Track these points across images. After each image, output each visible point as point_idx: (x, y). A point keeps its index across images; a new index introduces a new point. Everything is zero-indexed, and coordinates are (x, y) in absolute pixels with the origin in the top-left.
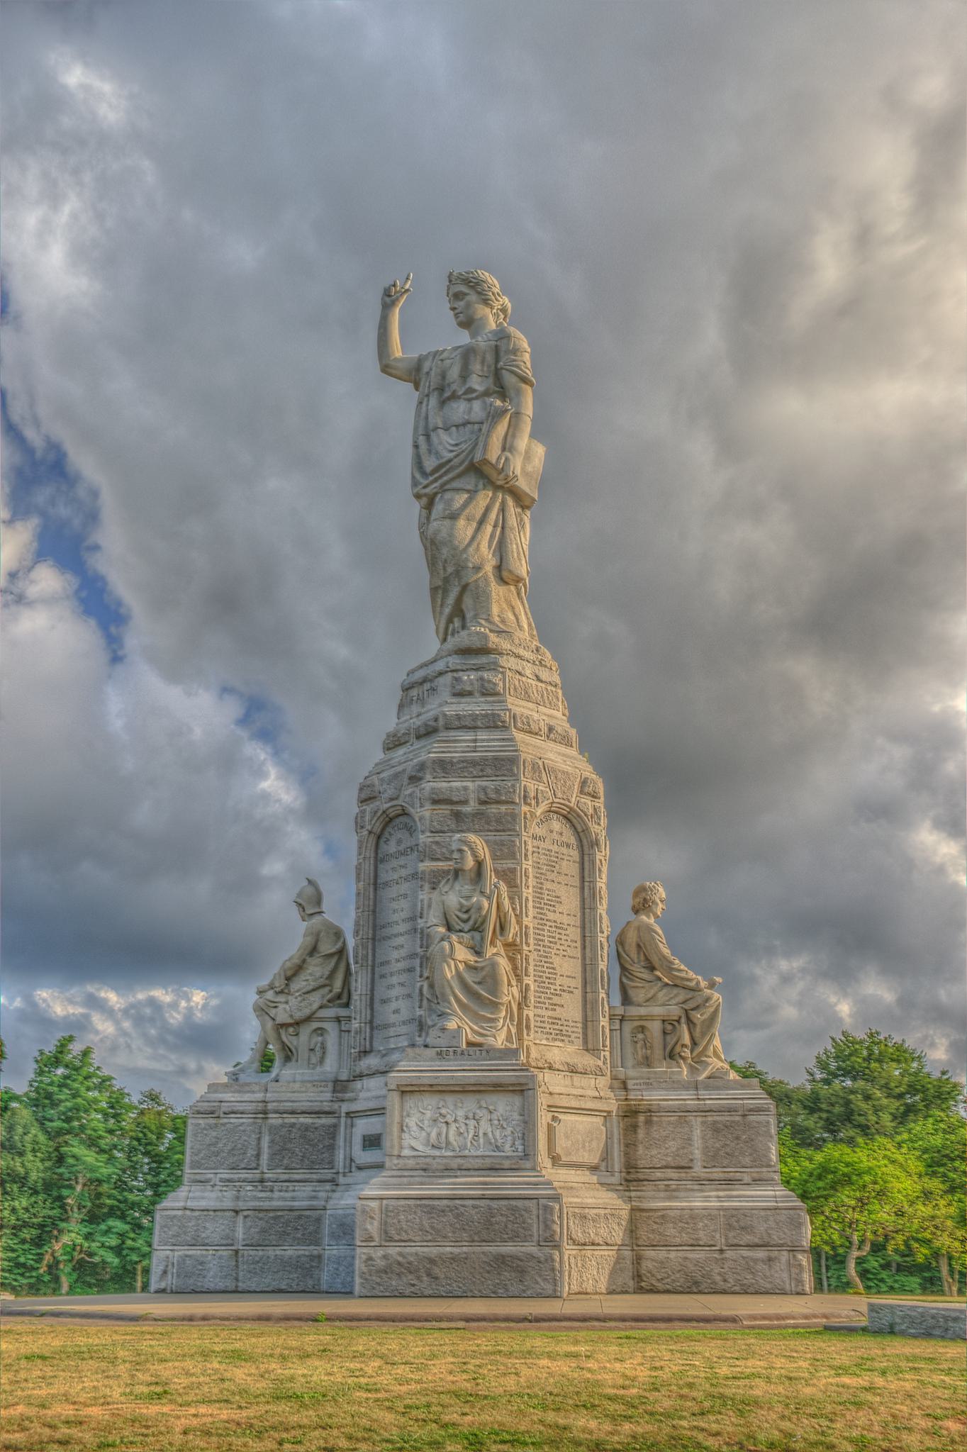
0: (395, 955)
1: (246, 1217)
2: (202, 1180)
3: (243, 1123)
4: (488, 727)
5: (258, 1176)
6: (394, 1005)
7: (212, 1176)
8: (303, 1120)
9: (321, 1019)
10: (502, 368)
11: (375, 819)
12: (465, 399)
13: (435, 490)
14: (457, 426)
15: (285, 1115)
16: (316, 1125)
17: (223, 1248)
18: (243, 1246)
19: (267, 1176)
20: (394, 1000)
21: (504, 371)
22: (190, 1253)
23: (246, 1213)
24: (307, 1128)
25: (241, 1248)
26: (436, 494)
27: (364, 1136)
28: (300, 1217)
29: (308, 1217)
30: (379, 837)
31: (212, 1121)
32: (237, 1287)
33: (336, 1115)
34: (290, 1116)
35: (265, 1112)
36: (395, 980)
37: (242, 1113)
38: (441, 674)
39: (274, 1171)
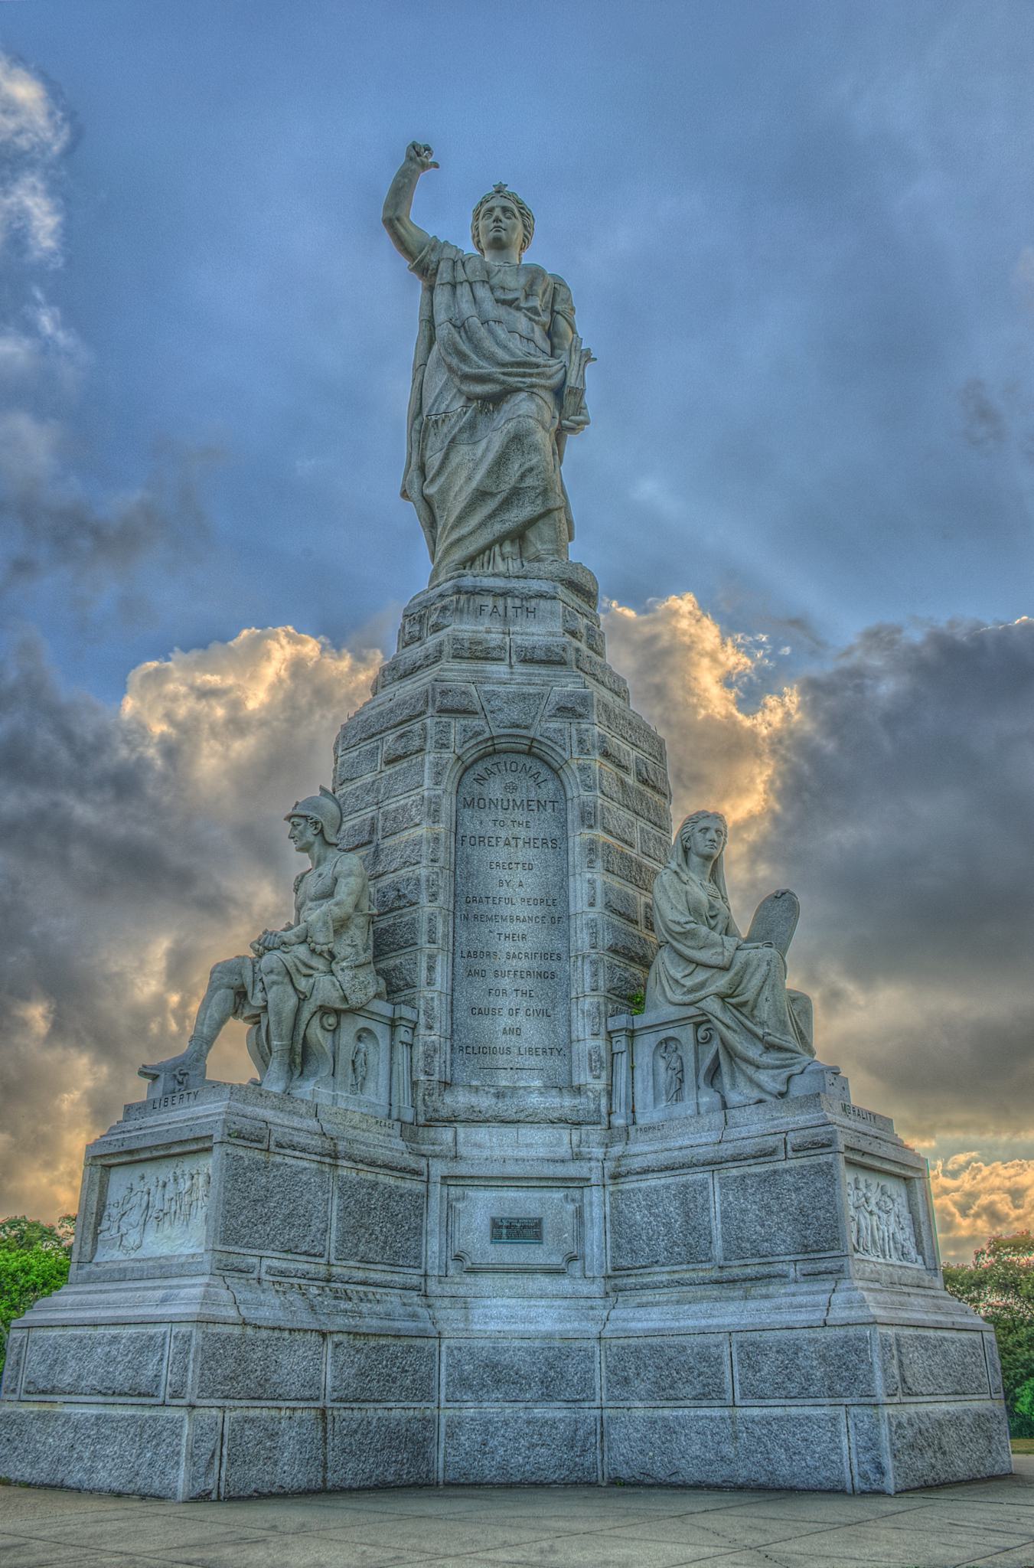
0: (507, 946)
1: (337, 1345)
2: (243, 1266)
3: (305, 1169)
4: (610, 689)
5: (323, 1270)
6: (505, 1021)
7: (255, 1260)
8: (387, 1179)
9: (372, 1015)
10: (558, 313)
11: (473, 742)
12: (526, 316)
13: (521, 385)
14: (521, 336)
15: (360, 1166)
16: (401, 1191)
17: (302, 1404)
18: (333, 1401)
19: (335, 1270)
20: (505, 1011)
21: (559, 317)
22: (252, 1413)
23: (336, 1338)
24: (391, 1193)
25: (329, 1405)
26: (519, 390)
27: (493, 1219)
28: (409, 1349)
29: (420, 1350)
30: (466, 769)
31: (260, 1156)
32: (324, 1480)
33: (424, 1178)
34: (366, 1168)
35: (335, 1156)
36: (506, 983)
37: (303, 1150)
38: (541, 596)
39: (344, 1263)
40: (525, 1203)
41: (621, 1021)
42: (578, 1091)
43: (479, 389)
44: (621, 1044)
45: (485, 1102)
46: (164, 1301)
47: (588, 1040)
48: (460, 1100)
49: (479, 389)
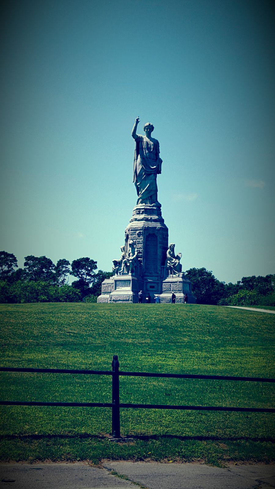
40: (153, 285)
41: (162, 266)
42: (158, 273)
43: (147, 173)
44: (162, 269)
45: (149, 274)
46: (128, 293)
47: (159, 268)
48: (146, 274)
49: (147, 173)
